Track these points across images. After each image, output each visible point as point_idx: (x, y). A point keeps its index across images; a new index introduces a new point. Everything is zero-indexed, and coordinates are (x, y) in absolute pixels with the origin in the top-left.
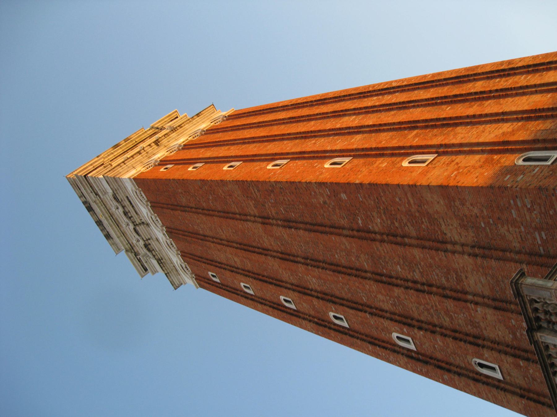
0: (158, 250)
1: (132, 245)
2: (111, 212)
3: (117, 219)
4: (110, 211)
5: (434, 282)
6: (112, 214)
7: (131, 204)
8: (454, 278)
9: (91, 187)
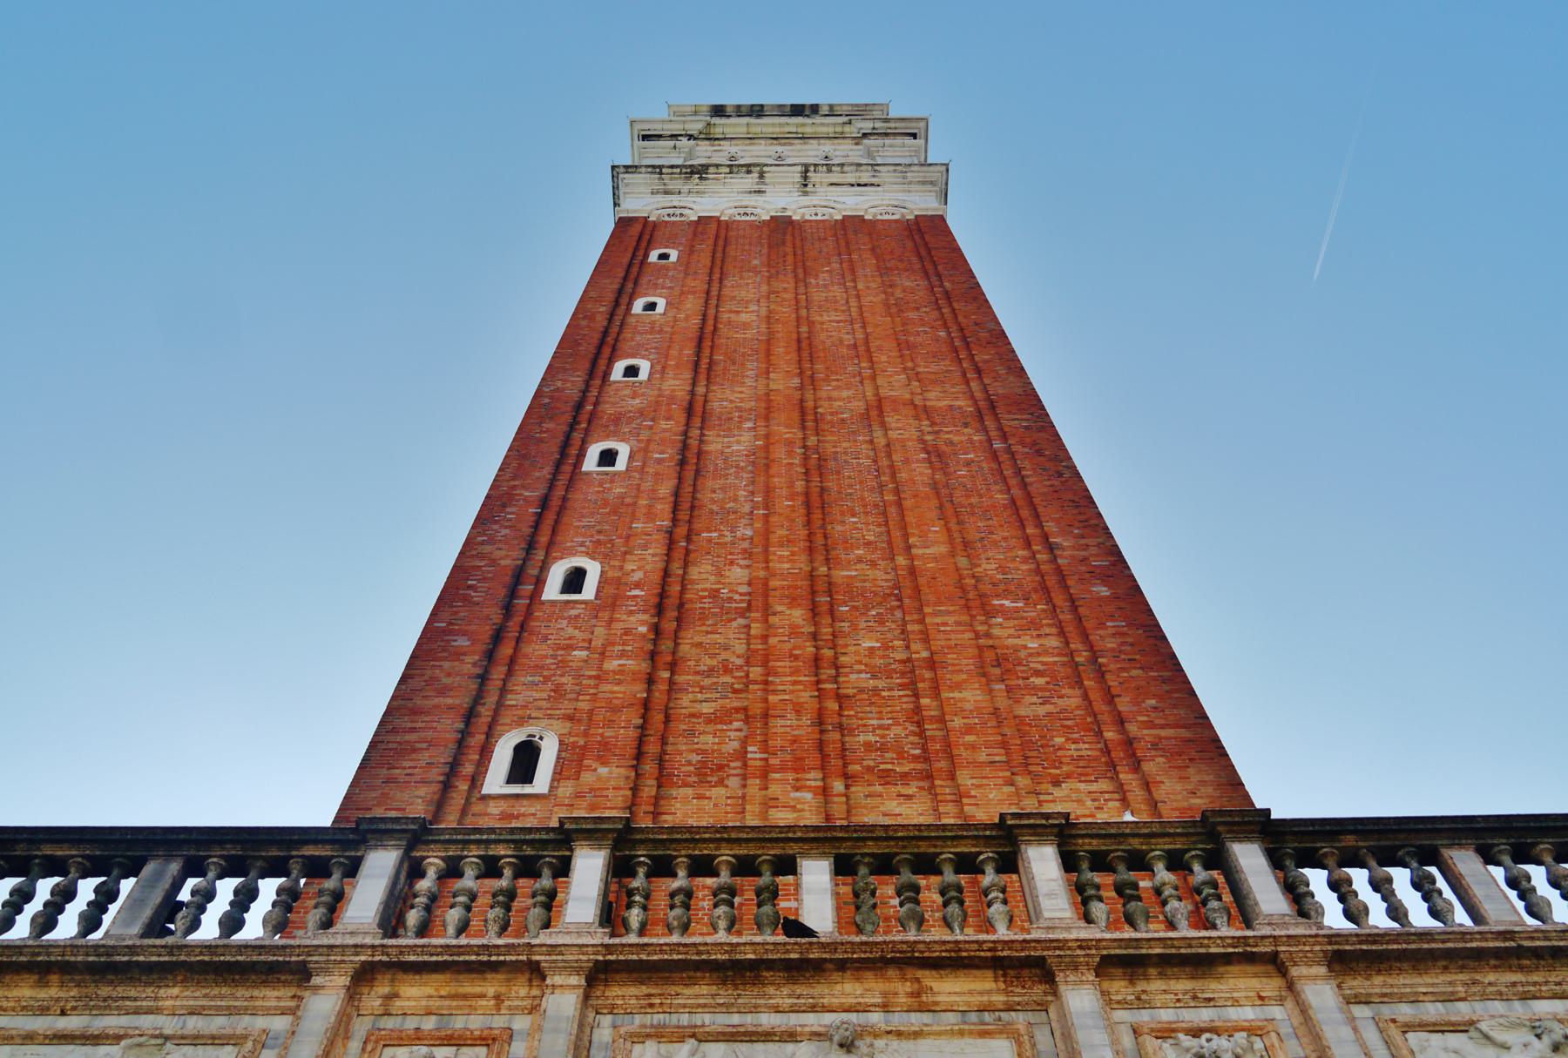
1: (716, 142)
2: (811, 141)
3: (792, 144)
5: (852, 713)
6: (806, 141)
7: (859, 185)
8: (889, 766)
9: (886, 134)
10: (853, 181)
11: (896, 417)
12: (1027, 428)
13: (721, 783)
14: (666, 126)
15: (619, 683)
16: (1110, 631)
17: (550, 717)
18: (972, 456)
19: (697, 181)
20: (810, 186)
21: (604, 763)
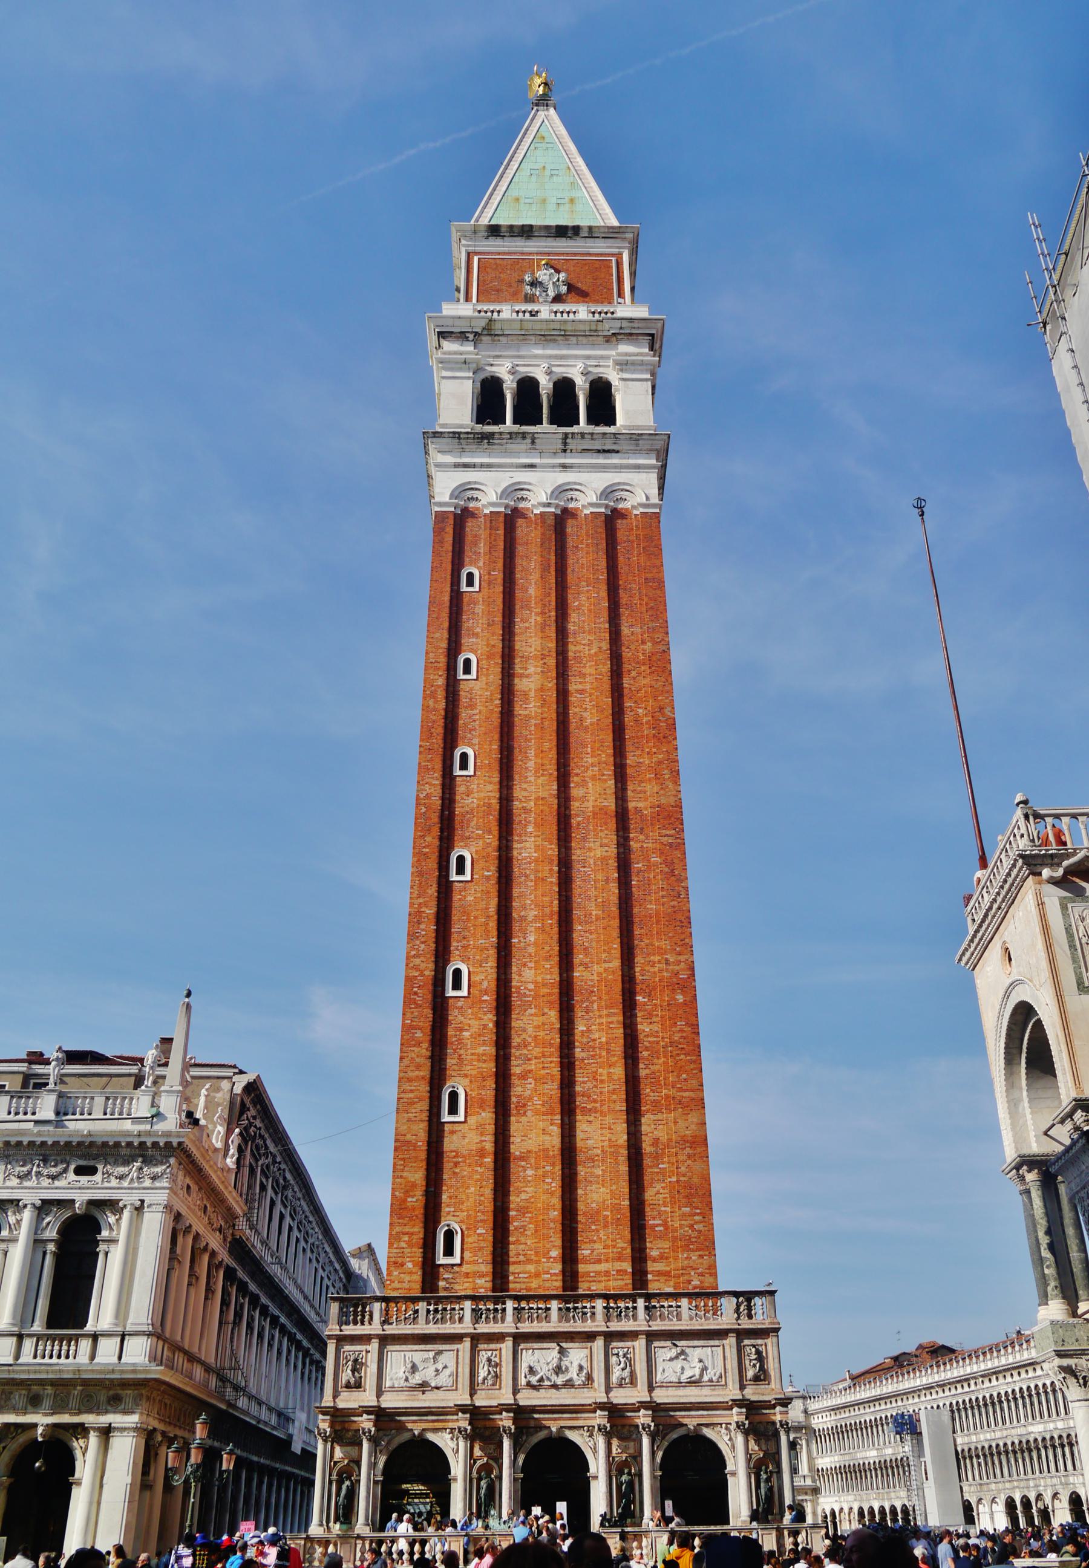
0: (509, 446)
1: (496, 338)
4: (574, 339)
7: (605, 451)
9: (631, 334)
10: (600, 448)
11: (606, 832)
12: (671, 845)
13: (524, 1114)
14: (458, 322)
15: (485, 1061)
16: (678, 1028)
17: (459, 1075)
18: (640, 865)
19: (486, 446)
20: (568, 451)
21: (484, 1110)
